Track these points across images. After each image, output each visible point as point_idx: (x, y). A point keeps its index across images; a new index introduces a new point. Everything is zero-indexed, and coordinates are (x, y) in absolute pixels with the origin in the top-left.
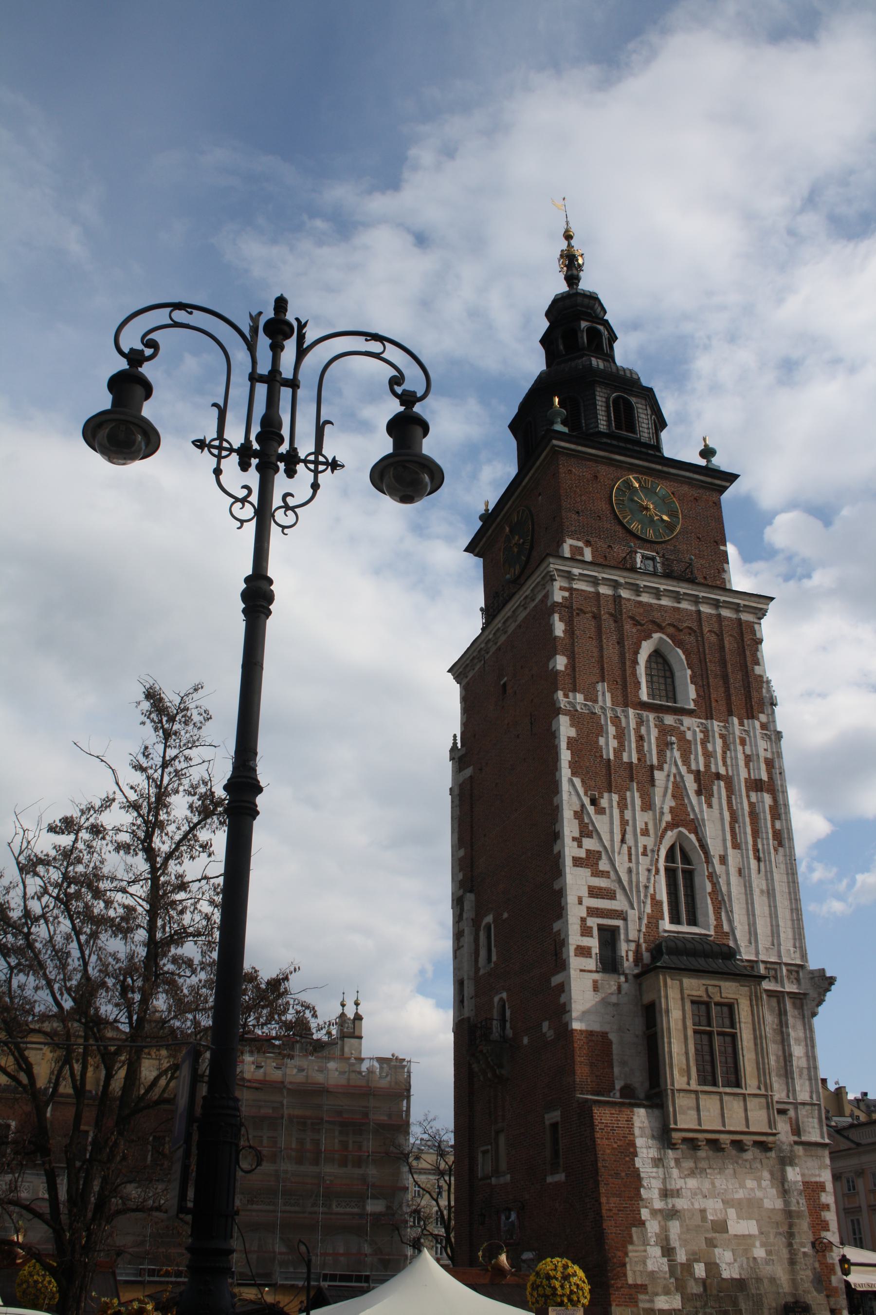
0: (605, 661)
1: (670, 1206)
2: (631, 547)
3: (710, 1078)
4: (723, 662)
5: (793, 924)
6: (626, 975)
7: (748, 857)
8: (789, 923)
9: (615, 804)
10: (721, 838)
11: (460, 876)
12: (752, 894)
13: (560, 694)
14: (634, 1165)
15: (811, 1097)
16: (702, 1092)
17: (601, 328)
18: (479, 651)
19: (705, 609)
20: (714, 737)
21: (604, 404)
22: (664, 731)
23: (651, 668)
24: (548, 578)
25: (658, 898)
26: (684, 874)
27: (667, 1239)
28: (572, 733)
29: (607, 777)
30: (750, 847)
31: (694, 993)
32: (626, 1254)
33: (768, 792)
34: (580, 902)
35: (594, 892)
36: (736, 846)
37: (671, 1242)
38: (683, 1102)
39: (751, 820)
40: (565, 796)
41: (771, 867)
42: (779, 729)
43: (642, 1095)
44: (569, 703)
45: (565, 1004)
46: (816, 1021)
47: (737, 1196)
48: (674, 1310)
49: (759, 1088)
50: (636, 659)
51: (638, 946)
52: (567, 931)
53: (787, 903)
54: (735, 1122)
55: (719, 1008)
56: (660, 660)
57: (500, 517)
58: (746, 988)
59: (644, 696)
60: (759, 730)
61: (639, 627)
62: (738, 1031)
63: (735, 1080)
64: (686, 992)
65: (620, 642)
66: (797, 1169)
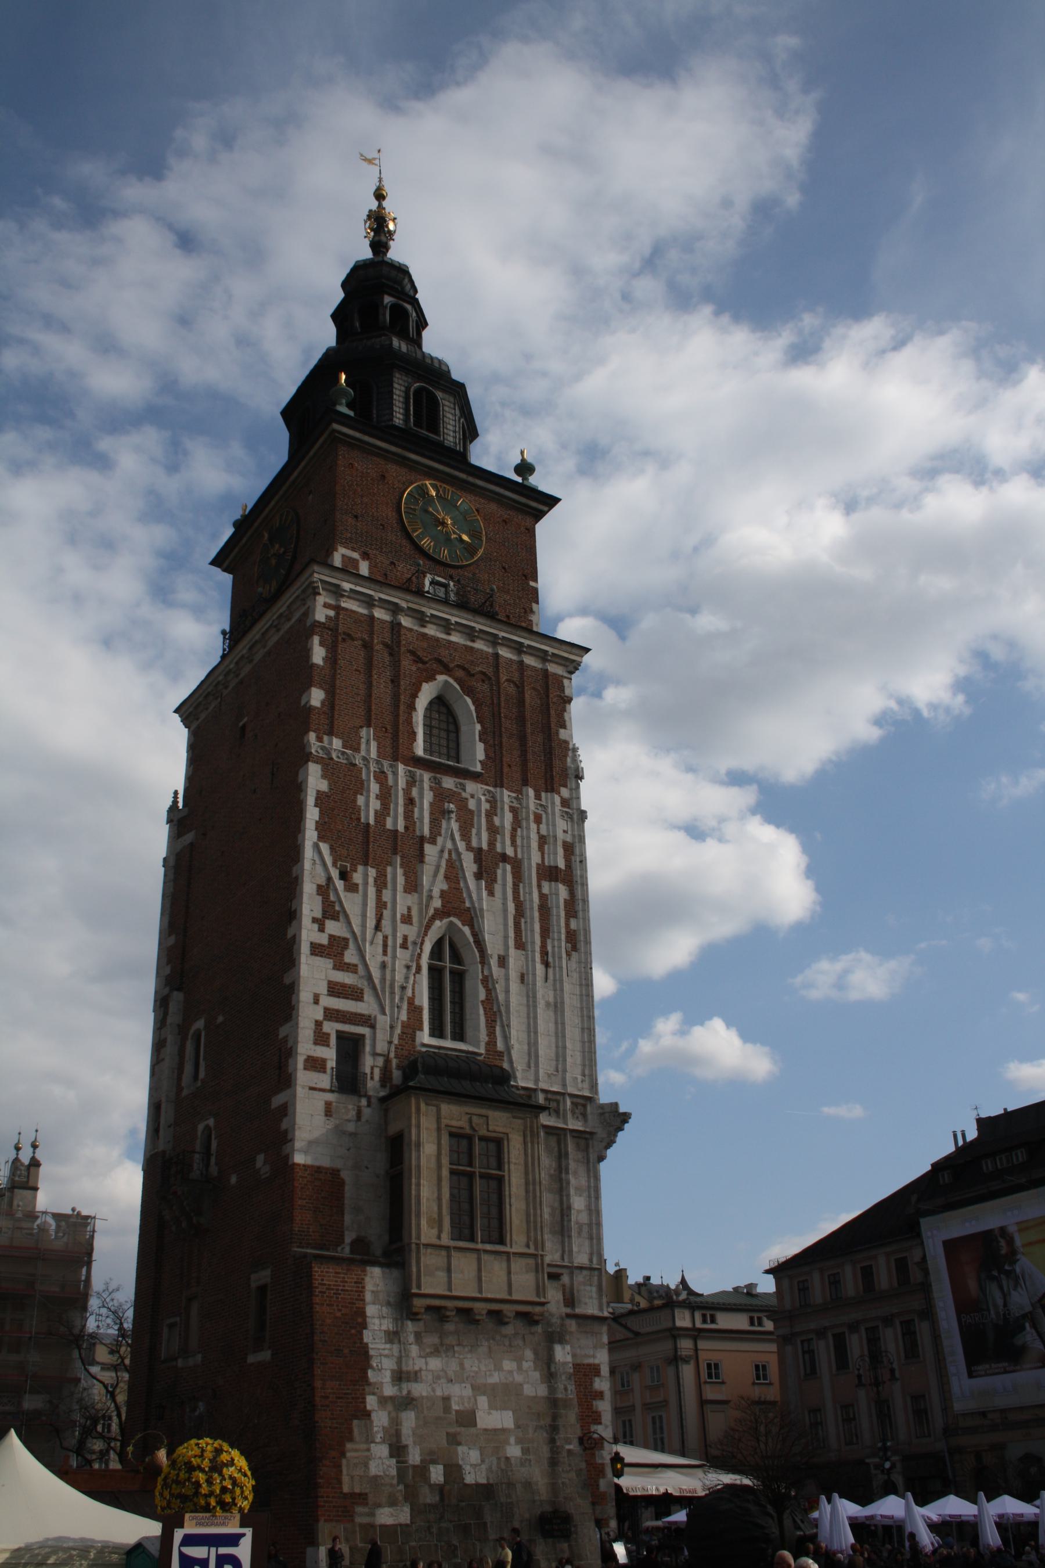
0: (374, 701)
1: (405, 1392)
2: (419, 565)
3: (466, 1232)
4: (521, 719)
5: (583, 1047)
6: (369, 1098)
7: (534, 961)
8: (578, 1045)
9: (371, 880)
10: (501, 934)
11: (167, 970)
12: (535, 1007)
13: (312, 736)
14: (362, 1339)
15: (591, 1260)
16: (455, 1248)
17: (409, 307)
18: (216, 686)
19: (504, 653)
20: (502, 809)
21: (402, 394)
22: (441, 796)
23: (431, 718)
24: (310, 590)
25: (417, 1003)
26: (452, 973)
27: (398, 1434)
28: (324, 786)
29: (361, 845)
30: (538, 949)
31: (454, 1123)
32: (343, 1454)
33: (564, 882)
34: (316, 1001)
35: (335, 990)
36: (520, 945)
37: (403, 1439)
38: (430, 1260)
39: (541, 915)
40: (307, 865)
41: (561, 976)
42: (583, 808)
43: (378, 1252)
44: (323, 748)
45: (286, 1132)
46: (603, 1166)
47: (491, 1381)
48: (401, 1525)
49: (528, 1246)
50: (413, 703)
51: (387, 1061)
52: (296, 1037)
53: (577, 1021)
54: (495, 1287)
55: (483, 1144)
56: (443, 710)
57: (259, 521)
58: (520, 1121)
59: (419, 749)
60: (558, 807)
61: (420, 665)
62: (506, 1174)
64: (444, 1122)
65: (395, 681)
66: (568, 1348)
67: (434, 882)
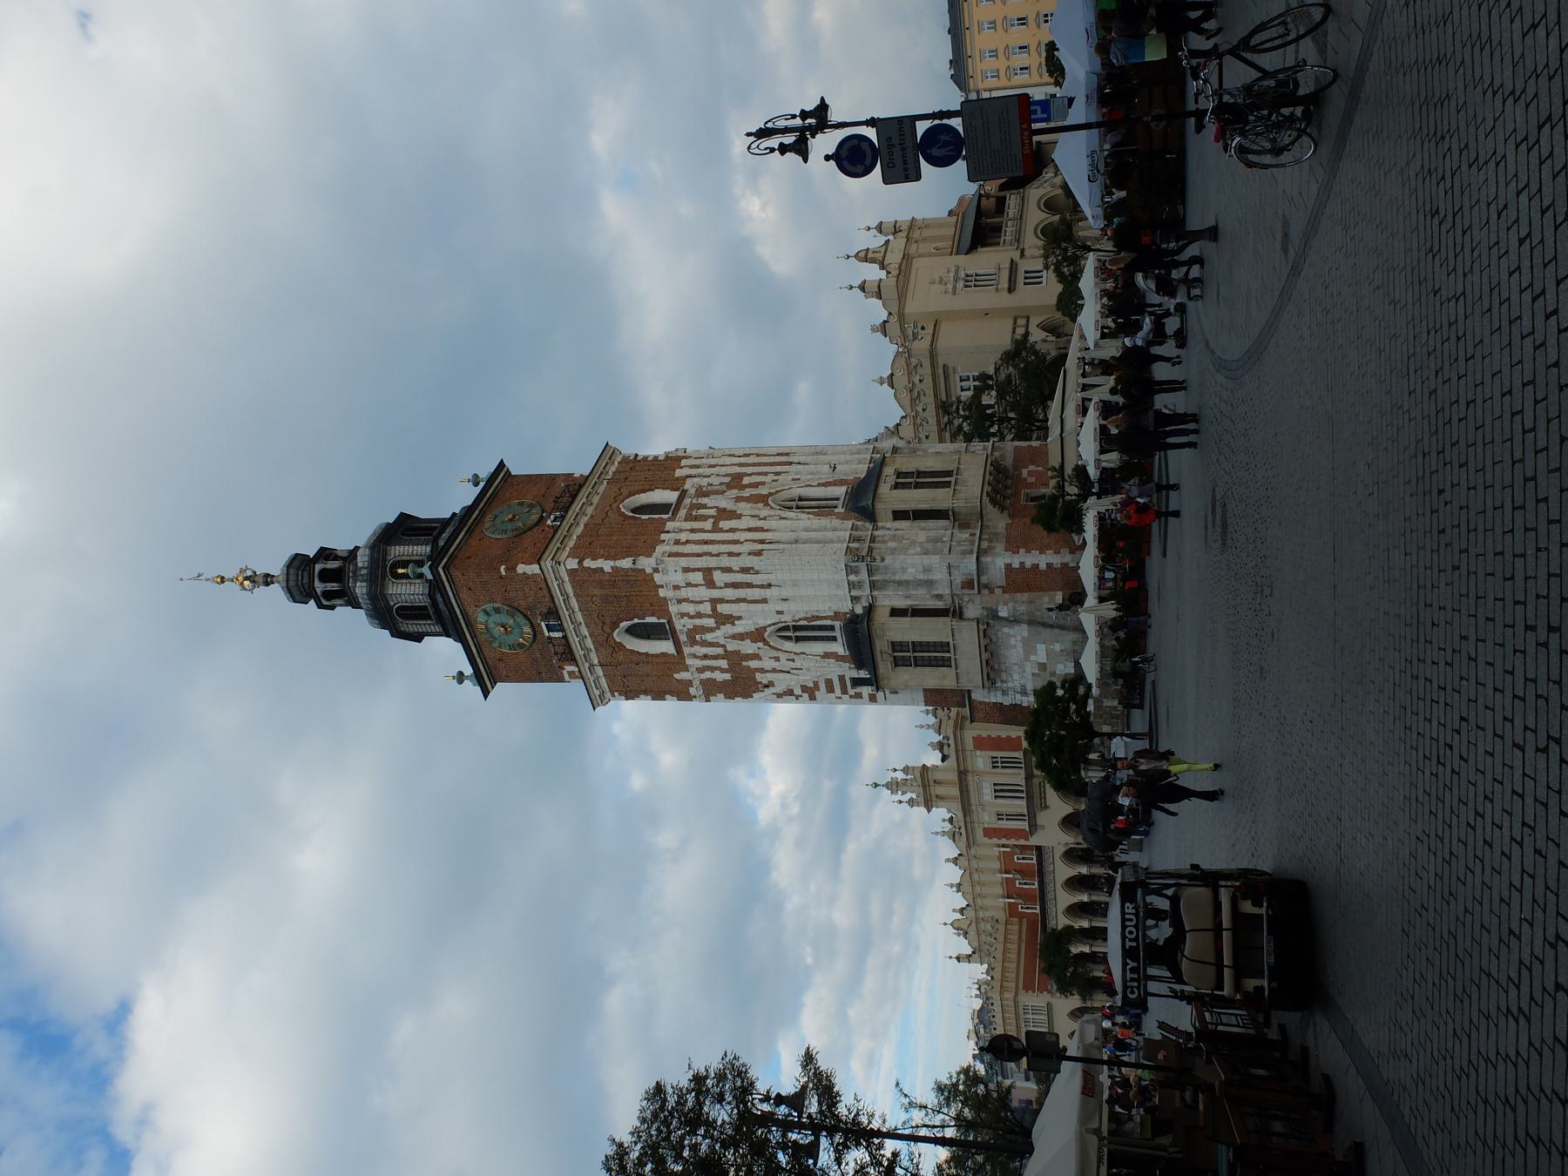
22: (693, 642)
36: (765, 601)
63: (944, 646)
67: (748, 647)
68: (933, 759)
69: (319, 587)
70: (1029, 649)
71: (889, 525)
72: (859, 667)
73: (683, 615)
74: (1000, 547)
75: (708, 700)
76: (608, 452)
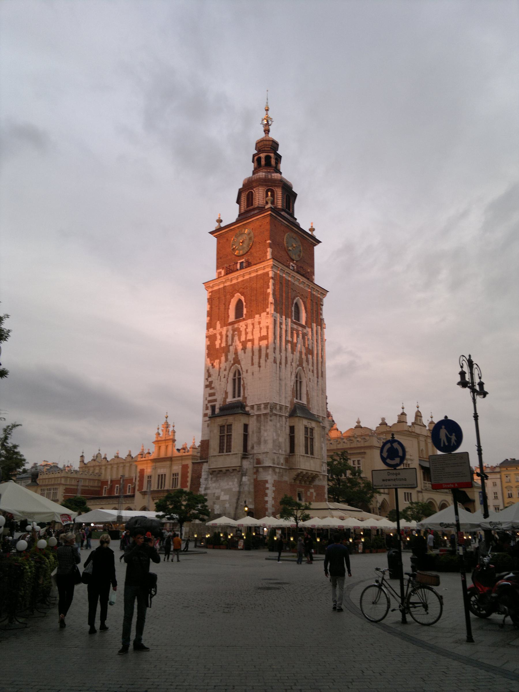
22: (234, 330)
36: (253, 364)
47: (226, 488)
63: (229, 450)
66: (247, 477)
67: (231, 356)
68: (179, 445)
69: (263, 155)
70: (227, 491)
71: (288, 424)
72: (221, 409)
73: (246, 326)
74: (276, 477)
75: (207, 337)
76: (324, 292)
